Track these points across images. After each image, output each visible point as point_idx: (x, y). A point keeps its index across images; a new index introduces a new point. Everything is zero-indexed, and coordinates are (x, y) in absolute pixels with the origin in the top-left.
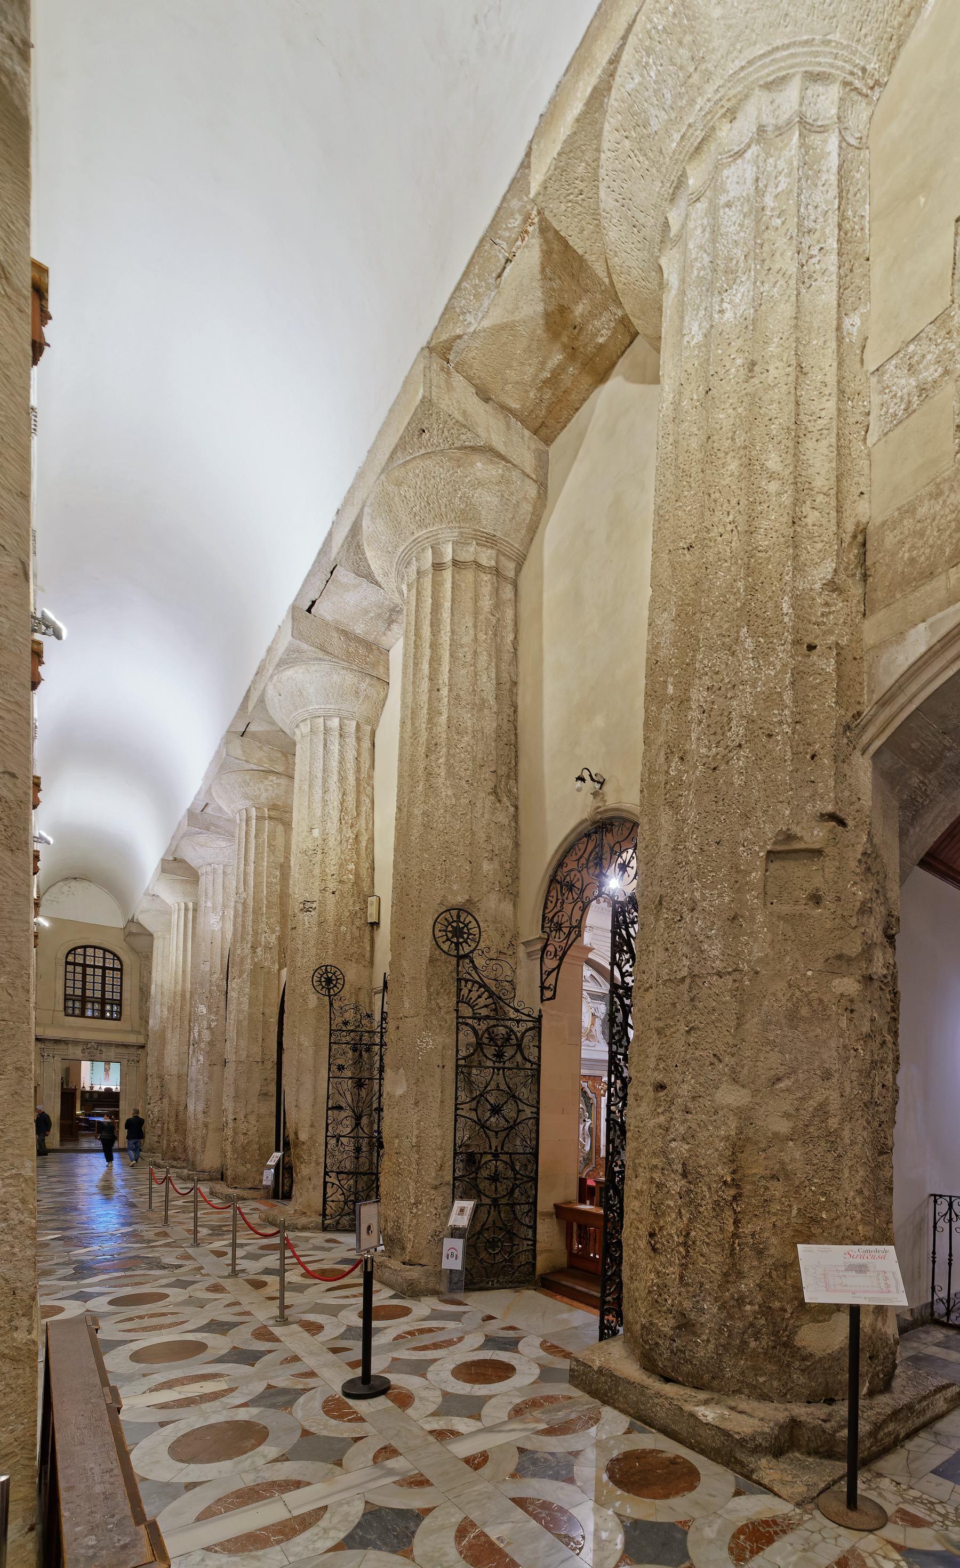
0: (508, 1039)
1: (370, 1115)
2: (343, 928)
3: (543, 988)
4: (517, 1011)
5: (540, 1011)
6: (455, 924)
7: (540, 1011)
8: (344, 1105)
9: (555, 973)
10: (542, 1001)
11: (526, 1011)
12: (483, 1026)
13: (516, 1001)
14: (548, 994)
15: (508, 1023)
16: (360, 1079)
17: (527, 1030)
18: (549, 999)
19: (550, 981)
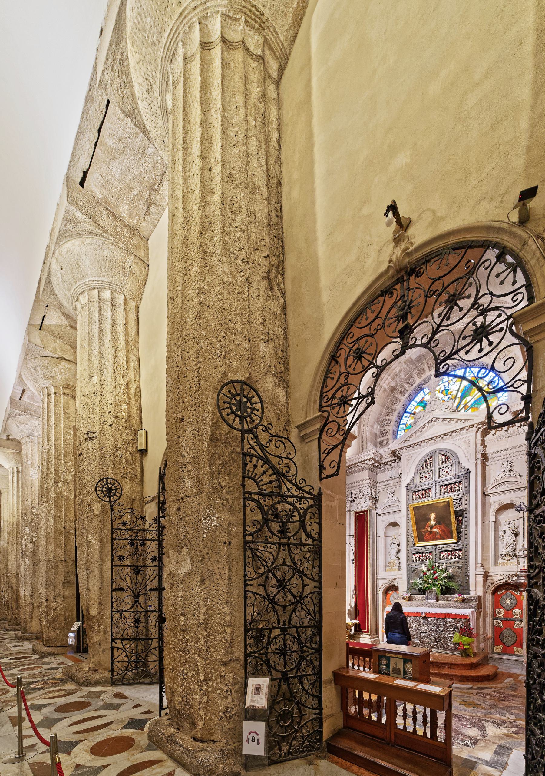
1: (145, 594)
3: (321, 467)
4: (300, 489)
5: (320, 489)
7: (320, 489)
8: (124, 587)
10: (321, 479)
11: (307, 489)
16: (137, 567)
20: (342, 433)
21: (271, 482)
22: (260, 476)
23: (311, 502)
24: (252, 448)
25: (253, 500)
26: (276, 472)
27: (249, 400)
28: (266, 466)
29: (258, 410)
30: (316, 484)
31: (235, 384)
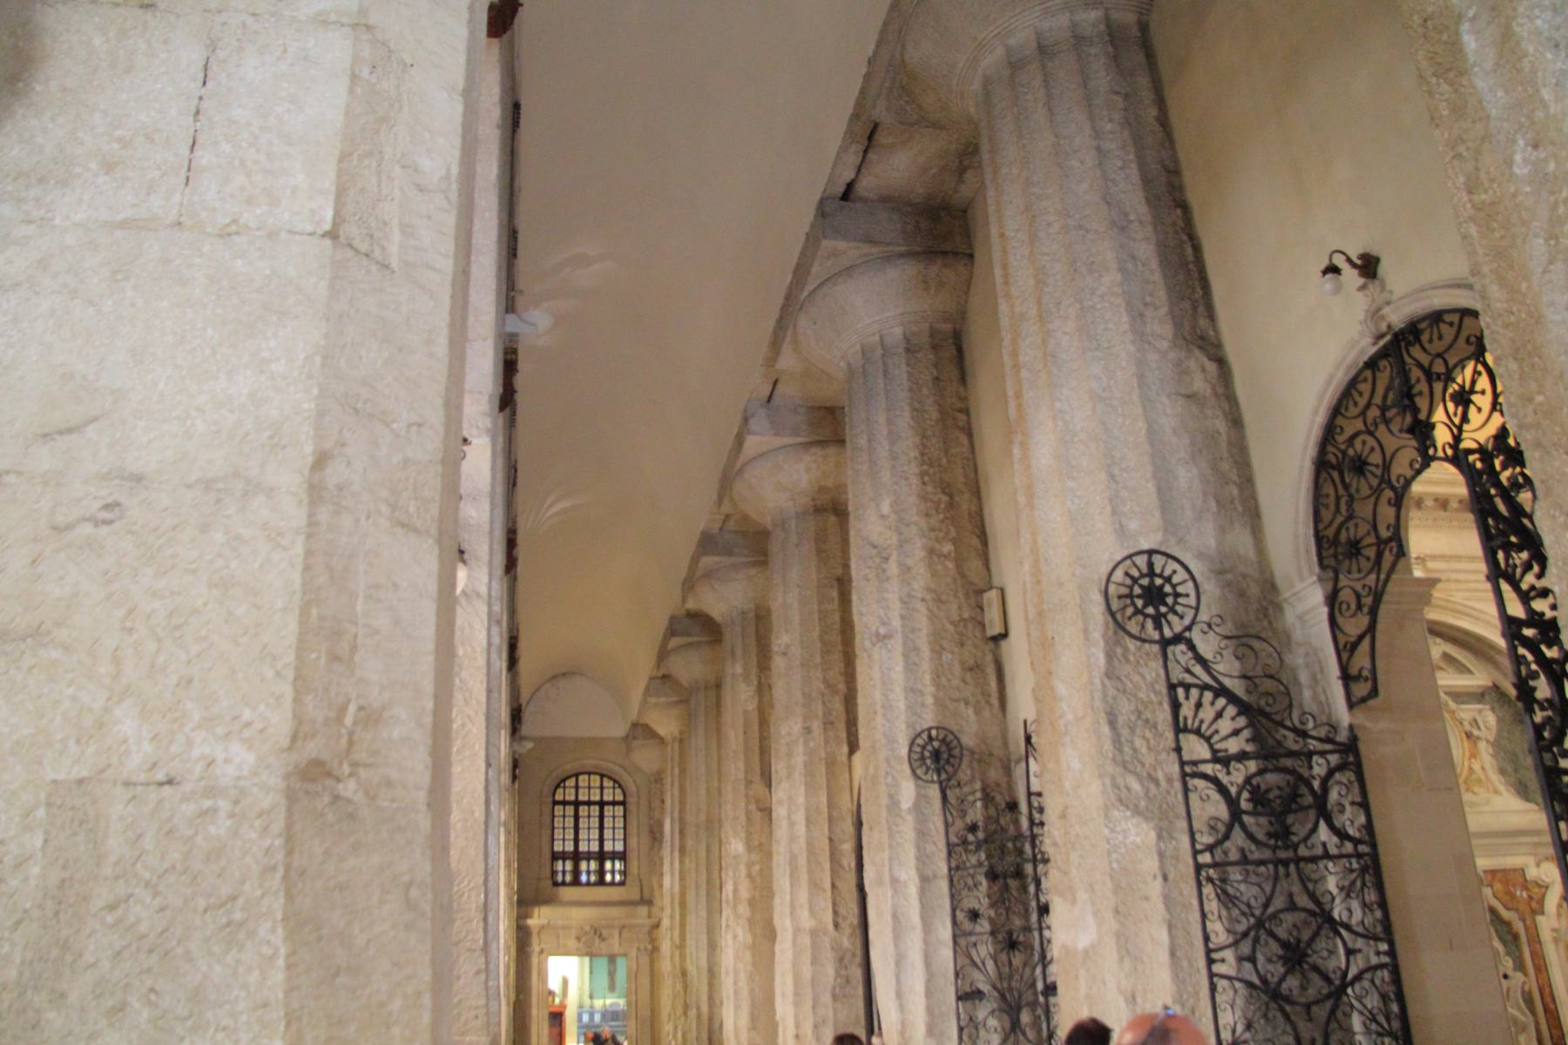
0: (1295, 796)
2: (947, 657)
3: (1347, 678)
6: (1140, 603)
9: (1365, 645)
10: (1351, 705)
12: (1235, 777)
13: (1295, 714)
14: (1361, 689)
15: (1287, 762)
17: (1331, 773)
18: (1363, 700)
19: (1361, 660)
20: (1366, 610)
21: (1236, 733)
22: (1212, 723)
23: (1334, 759)
24: (1188, 671)
25: (1205, 776)
26: (1244, 708)
27: (1168, 580)
28: (1221, 702)
29: (1187, 595)
30: (1343, 716)
31: (1134, 558)
